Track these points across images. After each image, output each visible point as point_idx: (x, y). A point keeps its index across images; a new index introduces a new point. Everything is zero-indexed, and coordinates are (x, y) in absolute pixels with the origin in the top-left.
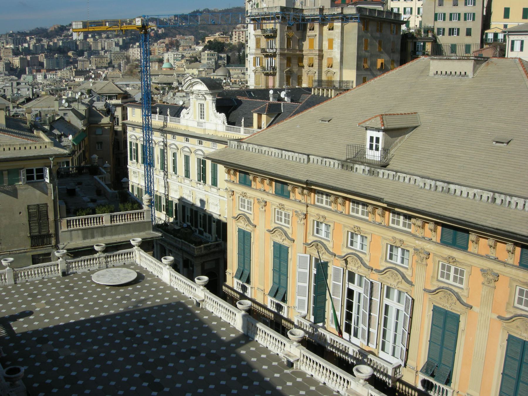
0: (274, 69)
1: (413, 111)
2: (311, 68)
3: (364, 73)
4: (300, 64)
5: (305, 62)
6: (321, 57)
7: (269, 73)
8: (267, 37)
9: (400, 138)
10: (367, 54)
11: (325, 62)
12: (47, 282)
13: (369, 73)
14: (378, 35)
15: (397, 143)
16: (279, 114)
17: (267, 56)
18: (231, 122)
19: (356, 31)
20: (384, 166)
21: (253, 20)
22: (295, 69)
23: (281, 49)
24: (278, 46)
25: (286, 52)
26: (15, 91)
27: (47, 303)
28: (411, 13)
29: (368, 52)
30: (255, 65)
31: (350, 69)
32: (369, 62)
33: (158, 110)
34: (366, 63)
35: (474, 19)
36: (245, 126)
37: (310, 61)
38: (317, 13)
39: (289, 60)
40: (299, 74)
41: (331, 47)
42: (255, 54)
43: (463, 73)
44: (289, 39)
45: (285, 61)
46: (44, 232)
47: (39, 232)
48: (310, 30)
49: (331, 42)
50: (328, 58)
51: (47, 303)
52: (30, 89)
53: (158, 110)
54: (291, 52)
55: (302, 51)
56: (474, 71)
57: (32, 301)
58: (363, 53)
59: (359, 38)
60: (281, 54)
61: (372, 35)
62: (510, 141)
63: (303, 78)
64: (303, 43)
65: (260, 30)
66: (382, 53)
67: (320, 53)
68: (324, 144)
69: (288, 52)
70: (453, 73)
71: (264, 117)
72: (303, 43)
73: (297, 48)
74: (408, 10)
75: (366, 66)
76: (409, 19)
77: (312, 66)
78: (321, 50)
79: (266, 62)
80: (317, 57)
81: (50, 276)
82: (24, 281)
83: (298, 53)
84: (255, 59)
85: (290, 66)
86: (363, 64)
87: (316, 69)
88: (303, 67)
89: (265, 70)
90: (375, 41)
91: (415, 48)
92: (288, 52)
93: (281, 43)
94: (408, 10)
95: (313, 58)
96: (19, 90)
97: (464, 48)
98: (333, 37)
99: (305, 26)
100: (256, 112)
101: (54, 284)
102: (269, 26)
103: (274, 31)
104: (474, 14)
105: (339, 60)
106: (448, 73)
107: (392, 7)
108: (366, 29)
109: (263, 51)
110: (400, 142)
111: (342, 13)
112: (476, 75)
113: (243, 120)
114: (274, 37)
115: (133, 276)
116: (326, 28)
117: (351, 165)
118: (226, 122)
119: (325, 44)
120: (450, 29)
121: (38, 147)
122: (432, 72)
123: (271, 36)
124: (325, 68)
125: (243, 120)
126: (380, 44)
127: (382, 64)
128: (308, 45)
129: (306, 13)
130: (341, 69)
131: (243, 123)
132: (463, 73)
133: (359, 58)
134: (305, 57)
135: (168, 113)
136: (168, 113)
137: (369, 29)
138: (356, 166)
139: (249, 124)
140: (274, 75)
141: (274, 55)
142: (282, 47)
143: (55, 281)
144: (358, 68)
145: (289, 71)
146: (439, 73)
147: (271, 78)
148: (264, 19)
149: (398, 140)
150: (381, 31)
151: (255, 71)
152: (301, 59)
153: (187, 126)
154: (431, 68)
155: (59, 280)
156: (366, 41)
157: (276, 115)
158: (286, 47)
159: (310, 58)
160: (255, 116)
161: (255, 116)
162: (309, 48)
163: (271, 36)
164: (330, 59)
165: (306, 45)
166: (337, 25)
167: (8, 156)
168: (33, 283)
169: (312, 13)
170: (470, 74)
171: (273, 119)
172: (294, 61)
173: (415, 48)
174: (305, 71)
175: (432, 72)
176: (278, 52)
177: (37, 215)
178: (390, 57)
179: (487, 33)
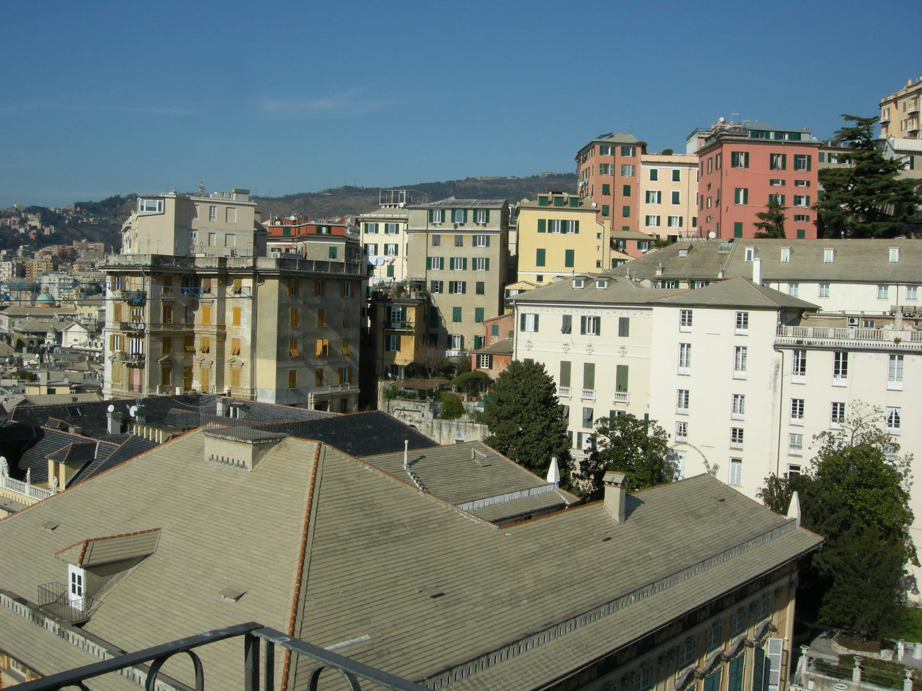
0: (141, 357)
1: (152, 527)
2: (206, 355)
3: (291, 365)
4: (188, 348)
5: (198, 344)
6: (222, 337)
7: (134, 362)
8: (130, 303)
9: (117, 575)
10: (296, 333)
11: (228, 346)
13: (301, 363)
14: (317, 300)
15: (112, 584)
16: (89, 462)
17: (130, 335)
18: (16, 473)
19: (275, 297)
20: (80, 625)
21: (110, 273)
22: (179, 357)
23: (152, 324)
24: (147, 319)
25: (162, 329)
28: (396, 253)
29: (298, 329)
30: (112, 349)
31: (267, 358)
32: (300, 347)
34: (295, 347)
35: (487, 268)
37: (204, 343)
38: (216, 265)
39: (167, 343)
40: (186, 364)
41: (237, 321)
42: (113, 330)
43: (241, 463)
44: (168, 309)
45: (161, 345)
48: (205, 292)
49: (237, 312)
50: (233, 339)
54: (172, 330)
55: (192, 326)
56: (255, 458)
58: (289, 331)
59: (282, 308)
60: (152, 334)
61: (305, 303)
62: (242, 595)
63: (194, 371)
64: (195, 312)
66: (325, 329)
67: (221, 331)
68: (32, 571)
69: (167, 329)
70: (230, 461)
71: (62, 467)
72: (195, 312)
73: (183, 321)
74: (391, 248)
75: (295, 353)
76: (393, 262)
77: (208, 351)
78: (221, 326)
79: (130, 346)
80: (215, 337)
83: (184, 329)
84: (113, 338)
85: (169, 352)
86: (289, 350)
87: (212, 356)
88: (194, 352)
89: (127, 358)
90: (311, 312)
91: (389, 317)
92: (167, 329)
93: (153, 315)
94: (391, 248)
95: (208, 338)
97: (473, 313)
98: (241, 306)
99: (198, 284)
100: (52, 458)
102: (135, 284)
103: (142, 295)
104: (487, 260)
105: (249, 343)
106: (225, 459)
107: (365, 242)
108: (294, 292)
109: (125, 326)
110: (117, 581)
111: (255, 266)
112: (256, 467)
113: (29, 472)
114: (142, 304)
116: (229, 290)
117: (41, 617)
118: (6, 472)
119: (229, 315)
120: (451, 283)
122: (207, 456)
123: (137, 300)
124: (228, 356)
125: (29, 472)
126: (321, 314)
127: (324, 347)
128: (201, 318)
129: (199, 264)
130: (253, 358)
132: (241, 463)
133: (282, 341)
134: (196, 336)
137: (301, 293)
138: (47, 620)
139: (40, 478)
140: (141, 366)
141: (141, 335)
142: (154, 322)
144: (280, 357)
145: (167, 360)
146: (215, 457)
147: (136, 371)
148: (128, 274)
149: (114, 578)
150: (322, 294)
151: (113, 359)
152: (189, 339)
154: (206, 449)
156: (295, 312)
157: (82, 465)
158: (162, 322)
159: (204, 339)
161: (51, 463)
162: (203, 323)
163: (137, 300)
164: (236, 341)
165: (198, 315)
166: (247, 283)
169: (209, 265)
170: (249, 464)
171: (78, 471)
172: (178, 344)
173: (389, 317)
174: (197, 357)
175: (207, 456)
176: (147, 329)
178: (341, 335)
179: (508, 291)
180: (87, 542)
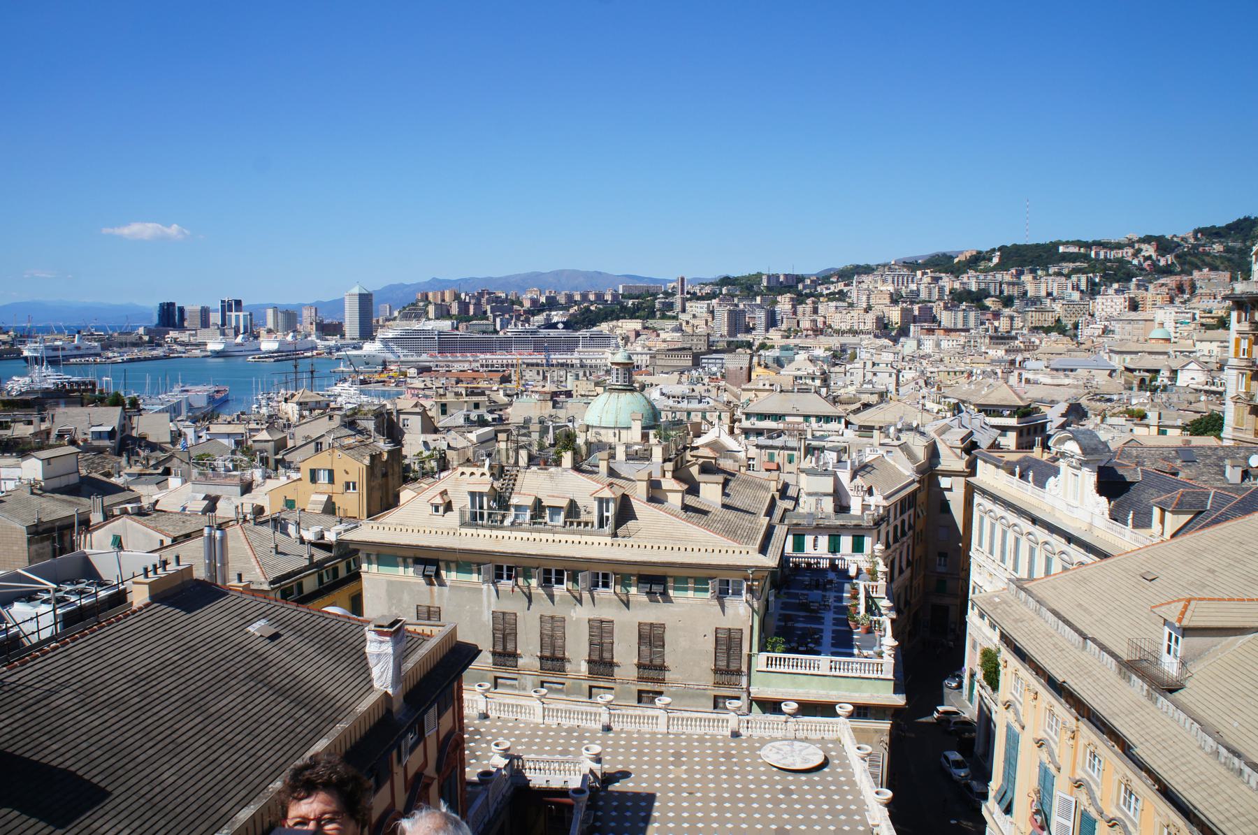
12: (707, 741)
16: (1201, 512)
26: (869, 376)
27: (686, 772)
33: (1017, 470)
36: (1135, 526)
46: (733, 666)
47: (728, 666)
51: (686, 772)
52: (894, 376)
53: (1017, 470)
57: (672, 763)
65: (1247, 324)
81: (715, 732)
82: (680, 731)
96: (875, 374)
101: (714, 747)
113: (1131, 515)
115: (818, 760)
118: (1107, 512)
121: (737, 552)
125: (1131, 515)
131: (1130, 522)
135: (1030, 479)
136: (1030, 479)
138: (1134, 677)
139: (1143, 522)
143: (719, 741)
153: (1053, 508)
155: (724, 741)
160: (1156, 512)
167: (694, 561)
168: (689, 739)
171: (1190, 516)
177: (727, 643)
180: (1189, 601)
